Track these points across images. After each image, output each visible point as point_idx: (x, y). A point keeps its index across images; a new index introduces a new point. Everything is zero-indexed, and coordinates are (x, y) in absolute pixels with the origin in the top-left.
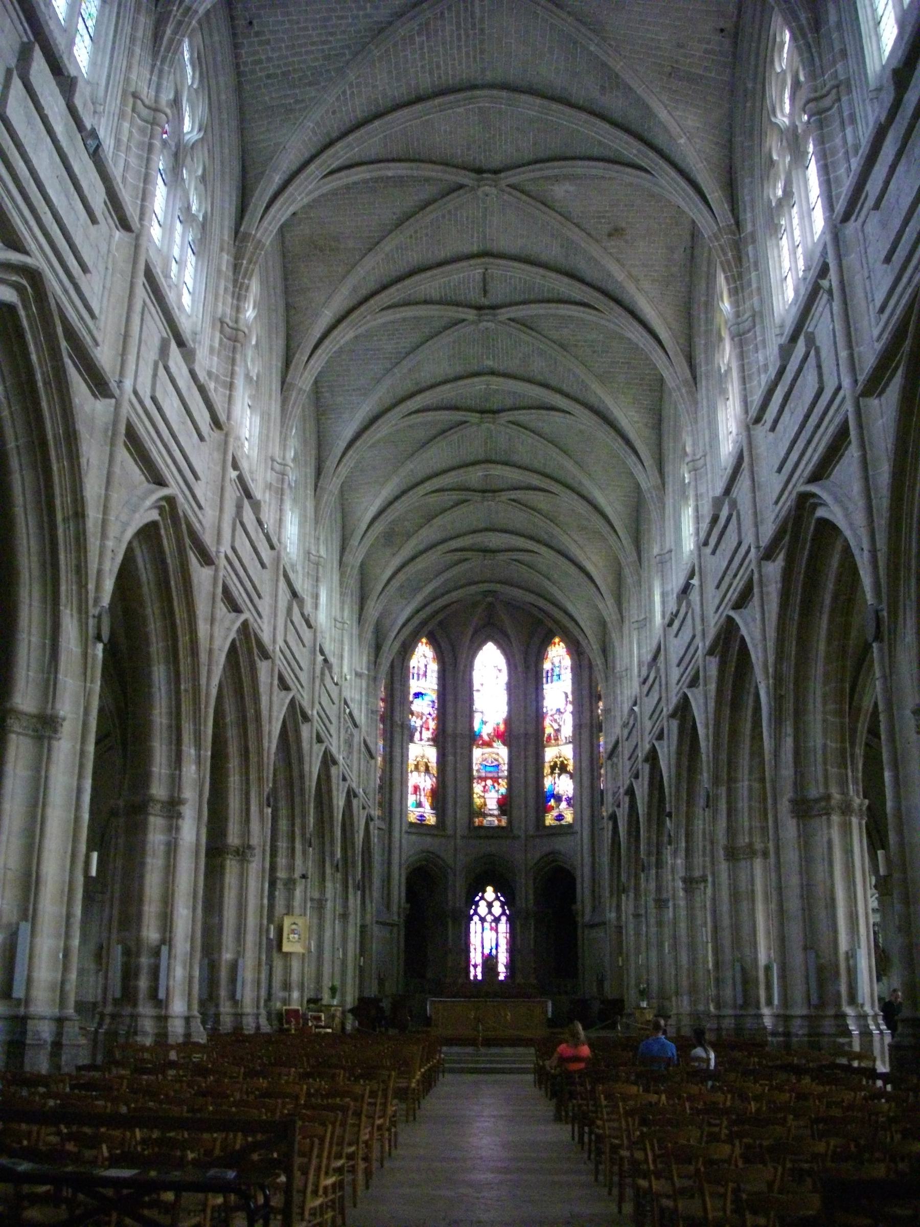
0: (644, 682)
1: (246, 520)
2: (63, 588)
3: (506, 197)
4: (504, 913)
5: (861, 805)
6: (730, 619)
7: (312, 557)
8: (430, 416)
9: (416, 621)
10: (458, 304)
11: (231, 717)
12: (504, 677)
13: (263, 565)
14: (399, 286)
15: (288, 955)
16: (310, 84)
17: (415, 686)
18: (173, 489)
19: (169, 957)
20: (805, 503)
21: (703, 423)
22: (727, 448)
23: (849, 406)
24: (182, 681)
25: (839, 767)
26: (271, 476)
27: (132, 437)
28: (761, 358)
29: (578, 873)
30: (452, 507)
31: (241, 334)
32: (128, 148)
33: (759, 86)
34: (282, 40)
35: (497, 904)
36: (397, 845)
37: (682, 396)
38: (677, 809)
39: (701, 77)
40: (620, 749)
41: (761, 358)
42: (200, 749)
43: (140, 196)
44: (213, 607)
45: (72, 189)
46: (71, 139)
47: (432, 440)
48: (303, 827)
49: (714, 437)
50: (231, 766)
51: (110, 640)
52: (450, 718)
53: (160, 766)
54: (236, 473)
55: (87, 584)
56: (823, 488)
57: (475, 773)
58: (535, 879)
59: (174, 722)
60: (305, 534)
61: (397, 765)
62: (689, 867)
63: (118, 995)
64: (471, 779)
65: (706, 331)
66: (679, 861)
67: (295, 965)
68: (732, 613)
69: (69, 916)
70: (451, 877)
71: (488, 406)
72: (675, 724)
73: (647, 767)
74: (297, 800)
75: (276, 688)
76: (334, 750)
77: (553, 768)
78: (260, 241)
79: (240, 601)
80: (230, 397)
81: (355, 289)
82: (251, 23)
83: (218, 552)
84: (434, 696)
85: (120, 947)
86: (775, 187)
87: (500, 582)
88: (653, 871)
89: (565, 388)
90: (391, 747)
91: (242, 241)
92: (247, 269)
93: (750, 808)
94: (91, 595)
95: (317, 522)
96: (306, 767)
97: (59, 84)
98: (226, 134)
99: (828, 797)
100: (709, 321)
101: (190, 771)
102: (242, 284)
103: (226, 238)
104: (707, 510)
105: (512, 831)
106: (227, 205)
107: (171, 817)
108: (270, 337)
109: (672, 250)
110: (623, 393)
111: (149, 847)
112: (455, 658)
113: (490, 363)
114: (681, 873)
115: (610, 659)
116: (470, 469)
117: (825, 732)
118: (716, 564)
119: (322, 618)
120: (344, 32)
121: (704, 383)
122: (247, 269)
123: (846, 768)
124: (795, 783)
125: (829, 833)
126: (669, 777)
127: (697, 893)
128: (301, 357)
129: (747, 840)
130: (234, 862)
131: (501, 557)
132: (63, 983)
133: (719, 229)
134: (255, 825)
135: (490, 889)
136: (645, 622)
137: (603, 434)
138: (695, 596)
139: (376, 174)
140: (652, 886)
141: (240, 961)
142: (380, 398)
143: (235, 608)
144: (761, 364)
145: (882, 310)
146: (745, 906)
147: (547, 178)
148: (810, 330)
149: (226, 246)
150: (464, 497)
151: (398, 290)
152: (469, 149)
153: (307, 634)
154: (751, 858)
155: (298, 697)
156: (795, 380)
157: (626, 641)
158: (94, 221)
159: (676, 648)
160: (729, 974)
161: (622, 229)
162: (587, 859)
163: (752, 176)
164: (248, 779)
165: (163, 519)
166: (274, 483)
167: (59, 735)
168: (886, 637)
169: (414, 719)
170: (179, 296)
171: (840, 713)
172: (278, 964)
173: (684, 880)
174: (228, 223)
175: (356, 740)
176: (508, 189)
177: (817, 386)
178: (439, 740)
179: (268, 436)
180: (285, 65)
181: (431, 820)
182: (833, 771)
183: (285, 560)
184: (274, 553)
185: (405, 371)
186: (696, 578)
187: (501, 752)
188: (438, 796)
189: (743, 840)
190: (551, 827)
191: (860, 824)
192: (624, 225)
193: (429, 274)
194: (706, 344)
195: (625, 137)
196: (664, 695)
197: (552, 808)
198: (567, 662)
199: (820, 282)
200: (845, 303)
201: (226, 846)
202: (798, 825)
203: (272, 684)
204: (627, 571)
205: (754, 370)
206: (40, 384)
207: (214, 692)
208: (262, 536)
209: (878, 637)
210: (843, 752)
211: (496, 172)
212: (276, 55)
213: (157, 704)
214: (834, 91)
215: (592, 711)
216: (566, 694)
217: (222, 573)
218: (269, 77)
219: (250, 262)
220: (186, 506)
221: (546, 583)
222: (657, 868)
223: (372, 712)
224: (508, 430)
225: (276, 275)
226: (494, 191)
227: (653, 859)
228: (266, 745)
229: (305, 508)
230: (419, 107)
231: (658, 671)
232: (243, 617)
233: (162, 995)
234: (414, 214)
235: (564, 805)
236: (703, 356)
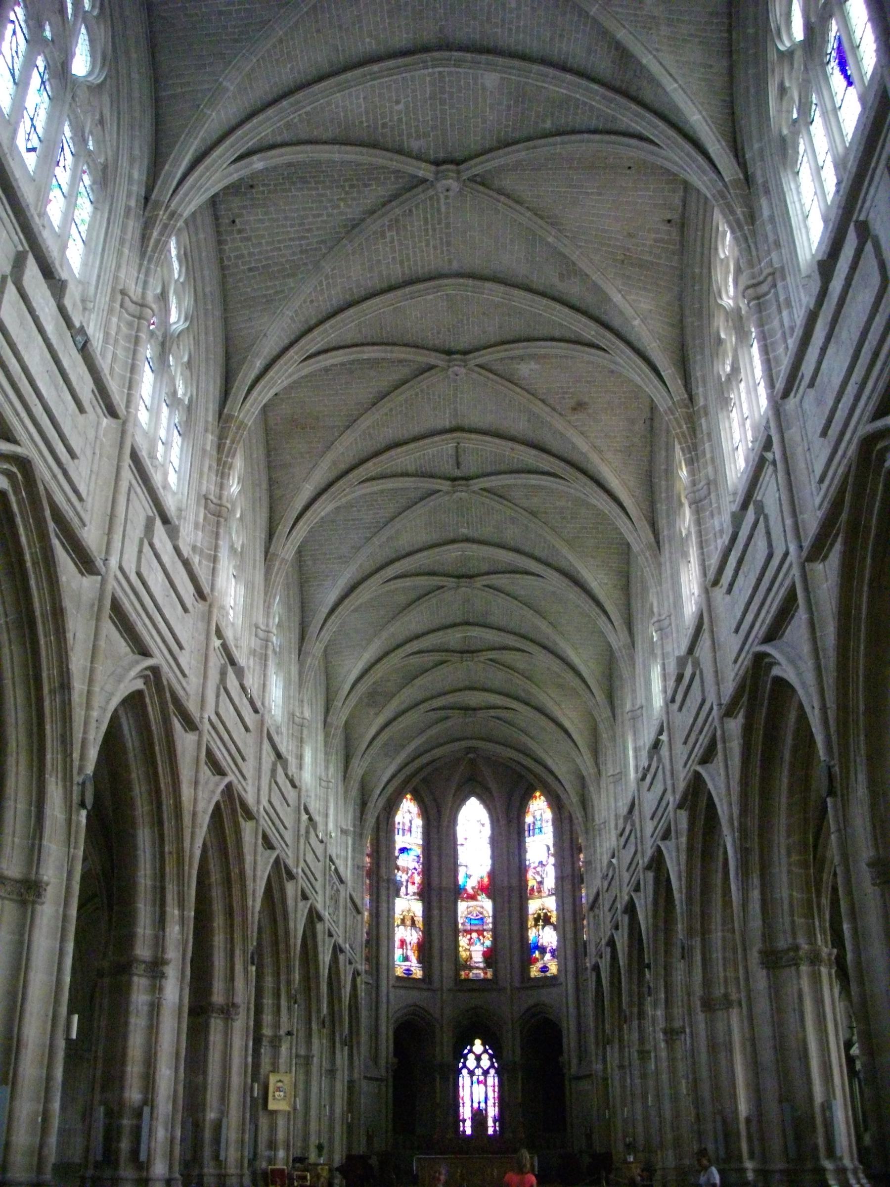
0: (621, 835)
1: (229, 686)
2: (49, 757)
3: (475, 376)
4: (492, 1066)
5: (830, 954)
6: (697, 776)
7: (296, 719)
8: (408, 582)
9: (401, 777)
10: (432, 476)
11: (215, 877)
12: (487, 831)
13: (247, 729)
14: (375, 460)
15: (274, 1113)
16: (289, 276)
17: (400, 841)
18: (159, 658)
19: (151, 1118)
20: (761, 662)
21: (667, 585)
22: (690, 608)
23: (796, 571)
24: (167, 842)
25: (805, 916)
26: (255, 643)
27: (117, 608)
28: (717, 523)
29: (564, 1025)
30: (433, 667)
31: (224, 510)
32: (116, 341)
33: (705, 271)
34: (263, 236)
35: (485, 1057)
36: (384, 999)
37: (647, 560)
38: (656, 960)
39: (652, 263)
40: (601, 901)
41: (717, 523)
42: (183, 910)
43: (127, 385)
44: (197, 772)
45: (62, 382)
46: (61, 336)
47: (409, 605)
48: (289, 983)
49: (678, 596)
50: (215, 925)
51: (93, 807)
52: (435, 872)
53: (144, 928)
54: (220, 642)
55: (71, 754)
56: (776, 648)
57: (460, 926)
58: (521, 1032)
59: (158, 884)
60: (289, 697)
61: (383, 919)
62: (669, 1017)
63: (99, 1158)
64: (456, 932)
65: (667, 498)
66: (659, 1013)
67: (281, 1122)
68: (699, 769)
69: (49, 1078)
71: (463, 571)
72: (650, 875)
73: (626, 918)
74: (283, 956)
75: (260, 848)
76: (319, 907)
77: (537, 920)
78: (242, 422)
79: (223, 764)
80: (214, 569)
81: (334, 463)
82: (234, 222)
83: (202, 718)
84: (418, 851)
85: (102, 1109)
86: (724, 364)
87: (482, 739)
88: (635, 1023)
89: (537, 553)
90: (378, 902)
91: (226, 421)
92: (230, 448)
93: (724, 958)
94: (76, 764)
95: (300, 686)
96: (291, 925)
97: (50, 287)
98: (210, 323)
99: (796, 948)
100: (670, 488)
101: (173, 931)
102: (225, 463)
103: (210, 419)
104: (672, 668)
105: (497, 983)
106: (211, 388)
107: (154, 978)
108: (254, 509)
109: (633, 422)
110: (592, 557)
111: (132, 1008)
112: (439, 812)
113: (464, 531)
114: (661, 1024)
115: (589, 810)
116: (449, 631)
117: (791, 885)
118: (683, 720)
119: (307, 777)
120: (318, 229)
121: (667, 546)
122: (230, 448)
123: (813, 918)
124: (764, 935)
125: (799, 984)
126: (647, 928)
127: (678, 1042)
128: (283, 528)
129: (722, 991)
130: (218, 1021)
131: (481, 714)
132: (42, 1146)
133: (674, 403)
134: (239, 983)
135: (478, 1042)
136: (620, 777)
137: (573, 595)
138: (664, 751)
139: (352, 357)
140: (635, 1035)
141: (224, 1120)
142: (361, 566)
143: (219, 771)
144: (717, 528)
145: (822, 480)
146: (722, 1056)
147: (512, 358)
148: (759, 498)
149: (210, 428)
150: (444, 658)
151: (375, 464)
152: (438, 333)
153: (291, 794)
154: (727, 1008)
155: (282, 855)
156: (747, 545)
157: (603, 795)
158: (81, 409)
159: (649, 801)
160: (709, 1126)
161: (585, 403)
162: (572, 1010)
163: (703, 354)
164: (232, 939)
165: (148, 689)
166: (258, 649)
167: (43, 899)
168: (839, 793)
169: (400, 873)
170: (165, 475)
171: (805, 865)
172: (264, 1122)
173: (665, 1032)
174: (213, 407)
175: (342, 894)
176: (477, 369)
177: (766, 553)
178: (424, 894)
179: (252, 604)
180: (267, 259)
181: (418, 973)
182: (800, 921)
183: (268, 721)
184: (258, 716)
185: (384, 539)
186: (665, 734)
187: (486, 905)
188: (424, 950)
189: (718, 991)
190: (536, 979)
191: (830, 974)
192: (586, 400)
193: (404, 448)
194: (668, 510)
195: (584, 319)
196: (639, 848)
197: (537, 960)
198: (548, 815)
199: (765, 454)
200: (788, 474)
201: (210, 1004)
202: (768, 975)
203: (256, 844)
204: (601, 727)
205: (711, 535)
206: (29, 564)
207: (198, 853)
208: (246, 701)
209: (831, 792)
210: (809, 902)
211: (465, 353)
212: (256, 251)
213: (141, 865)
214: (770, 279)
215: (573, 864)
216: (549, 849)
217: (206, 737)
218: (250, 270)
219: (233, 442)
220: (171, 675)
221: (524, 739)
222: (639, 1019)
223: (358, 867)
224: (484, 594)
225: (259, 452)
226: (463, 371)
227: (635, 1010)
228: (250, 903)
229: (289, 673)
230: (391, 295)
231: (633, 825)
232: (226, 780)
233: (143, 1157)
234: (388, 394)
235: (548, 956)
236: (664, 521)
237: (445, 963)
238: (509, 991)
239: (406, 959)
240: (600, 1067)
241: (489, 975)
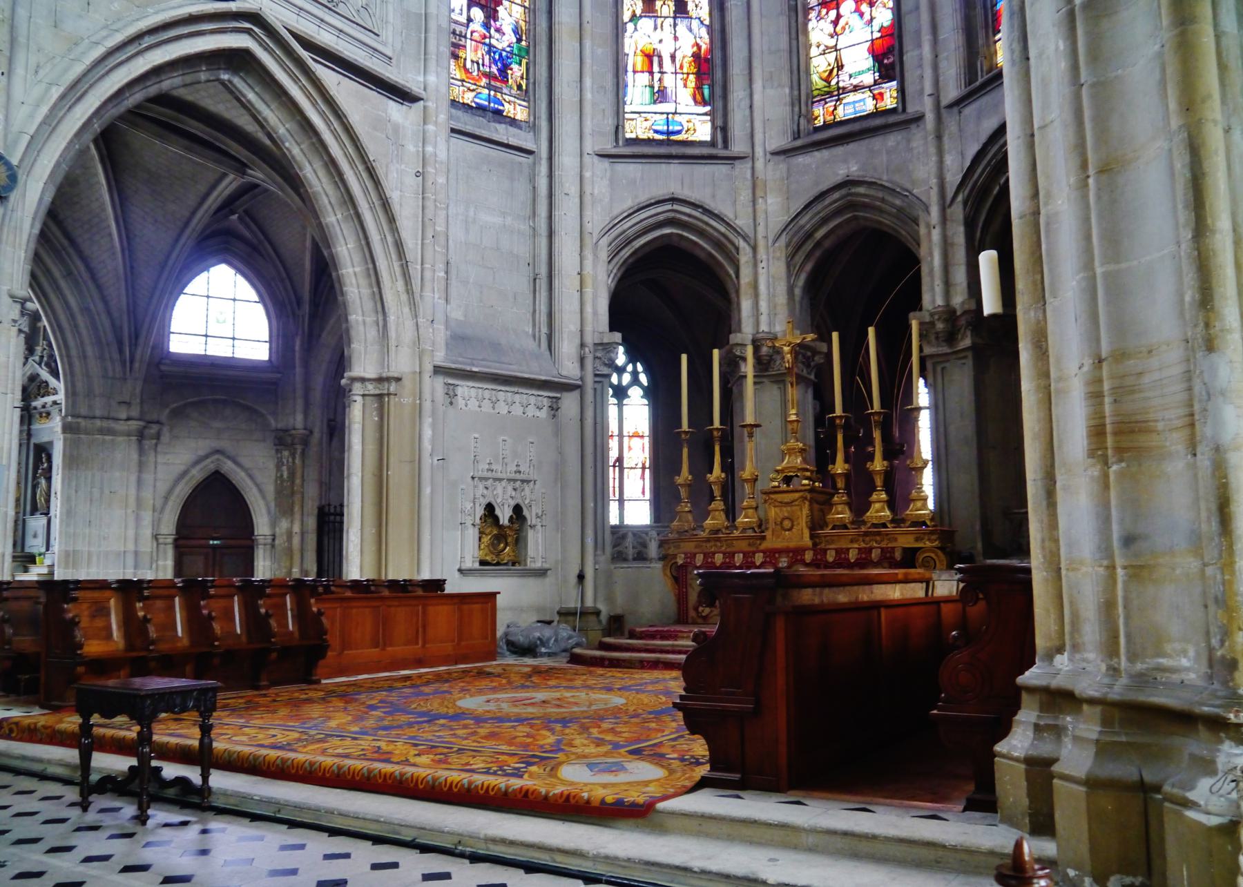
70: (745, 257)
181: (702, 131)
237: (758, 86)
238: (930, 117)
239: (660, 95)
241: (889, 102)
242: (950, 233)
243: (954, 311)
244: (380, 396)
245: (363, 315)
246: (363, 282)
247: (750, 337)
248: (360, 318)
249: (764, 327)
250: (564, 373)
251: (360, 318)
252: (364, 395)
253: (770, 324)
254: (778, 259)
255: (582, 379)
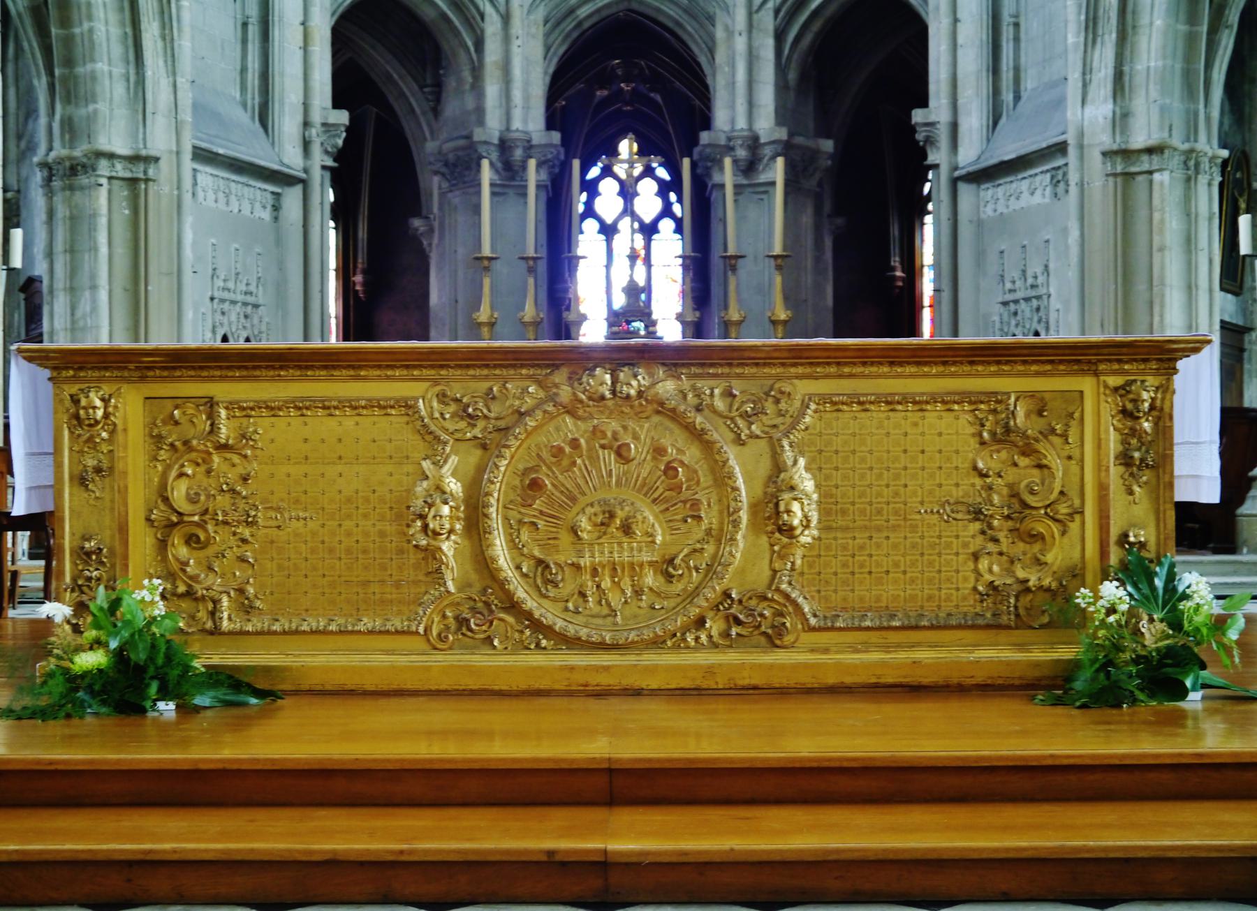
4: (667, 212)
35: (647, 188)
58: (779, 36)
70: (492, 26)
240: (1100, 110)
242: (756, 44)
243: (756, 138)
244: (133, 182)
245: (110, 65)
246: (113, 17)
247: (497, 134)
248: (106, 68)
249: (517, 124)
250: (286, 161)
251: (106, 68)
252: (110, 178)
253: (525, 121)
254: (533, 37)
255: (306, 171)
